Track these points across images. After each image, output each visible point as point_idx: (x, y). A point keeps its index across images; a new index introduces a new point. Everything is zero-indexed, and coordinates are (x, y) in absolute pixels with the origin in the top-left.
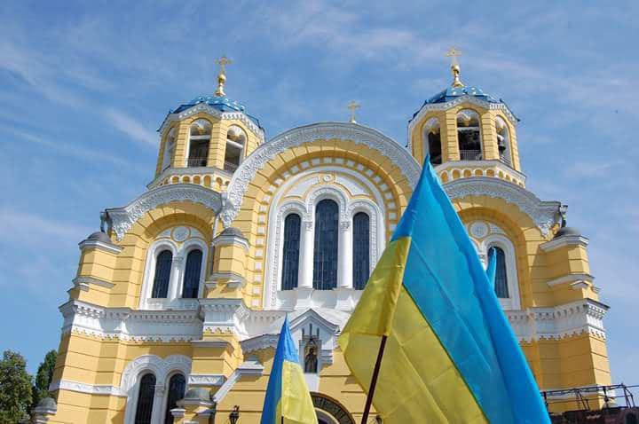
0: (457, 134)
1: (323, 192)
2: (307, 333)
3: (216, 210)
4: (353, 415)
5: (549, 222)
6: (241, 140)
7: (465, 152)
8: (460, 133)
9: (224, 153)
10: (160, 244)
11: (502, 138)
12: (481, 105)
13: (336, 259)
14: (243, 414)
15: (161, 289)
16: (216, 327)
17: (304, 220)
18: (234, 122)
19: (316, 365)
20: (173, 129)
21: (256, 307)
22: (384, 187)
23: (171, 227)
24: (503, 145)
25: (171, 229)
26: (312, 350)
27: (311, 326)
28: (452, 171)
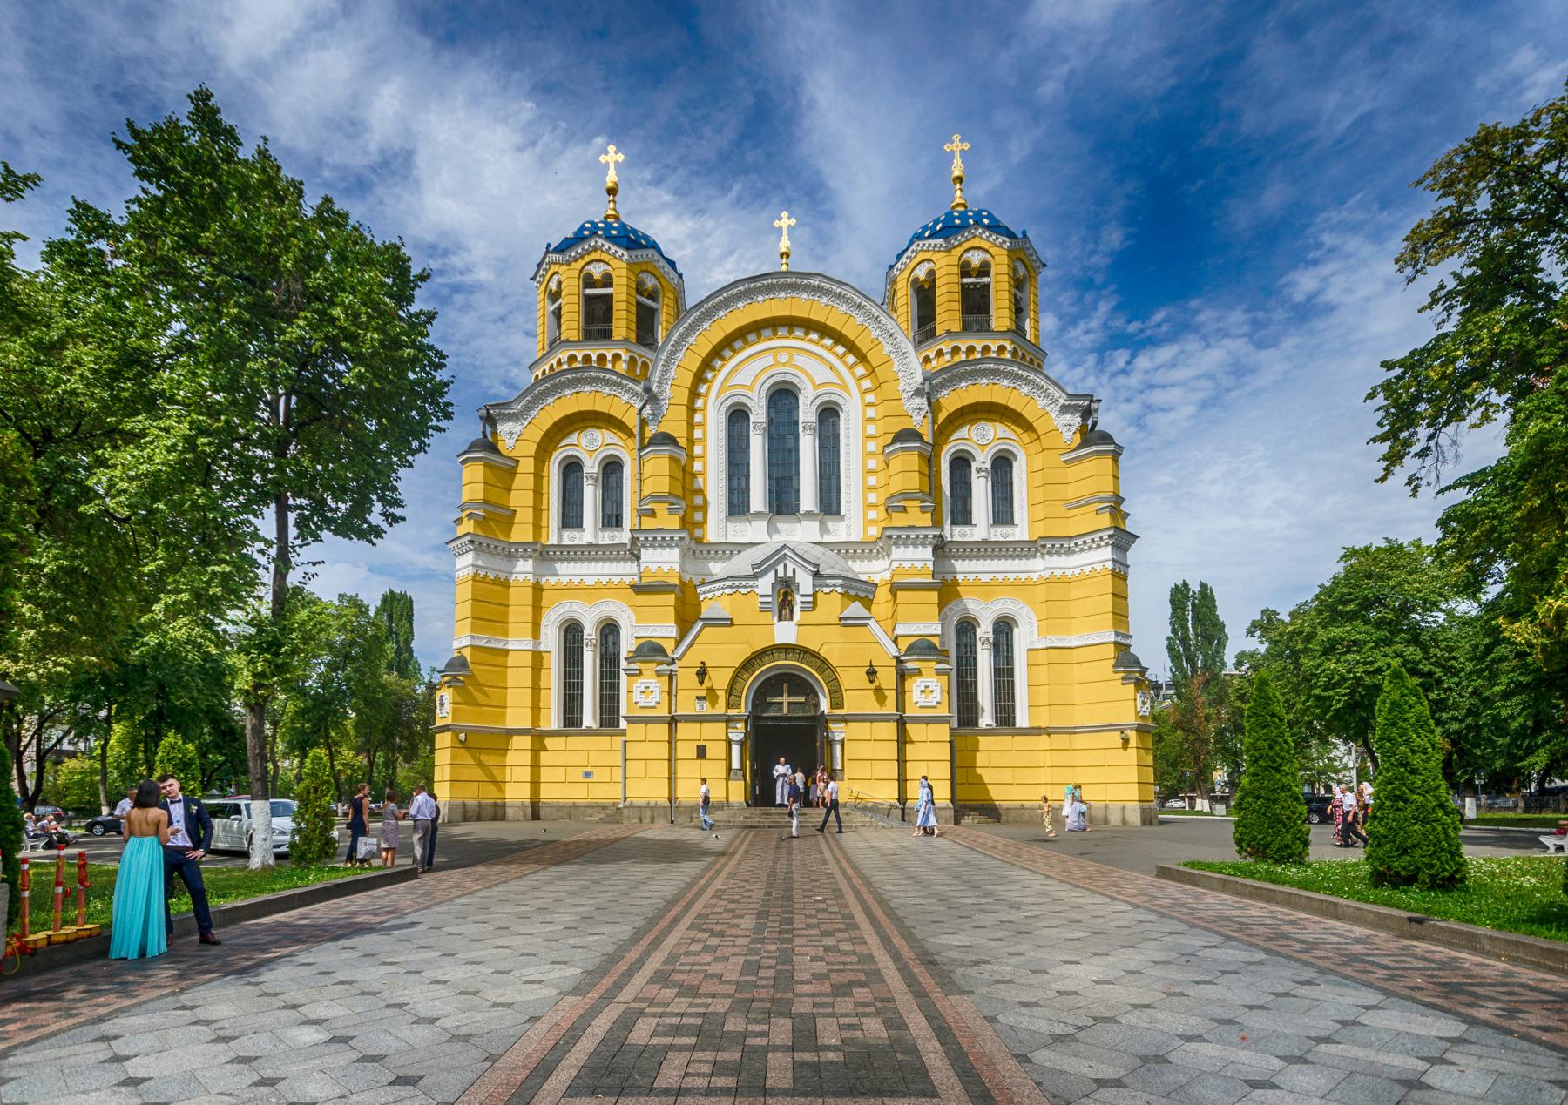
0: (957, 288)
2: (781, 574)
3: (638, 406)
5: (1077, 420)
6: (653, 296)
7: (969, 317)
8: (966, 291)
10: (564, 455)
11: (1019, 294)
13: (798, 474)
15: (571, 518)
16: (656, 566)
17: (752, 419)
18: (644, 268)
19: (792, 611)
20: (556, 277)
22: (860, 370)
23: (576, 430)
26: (786, 594)
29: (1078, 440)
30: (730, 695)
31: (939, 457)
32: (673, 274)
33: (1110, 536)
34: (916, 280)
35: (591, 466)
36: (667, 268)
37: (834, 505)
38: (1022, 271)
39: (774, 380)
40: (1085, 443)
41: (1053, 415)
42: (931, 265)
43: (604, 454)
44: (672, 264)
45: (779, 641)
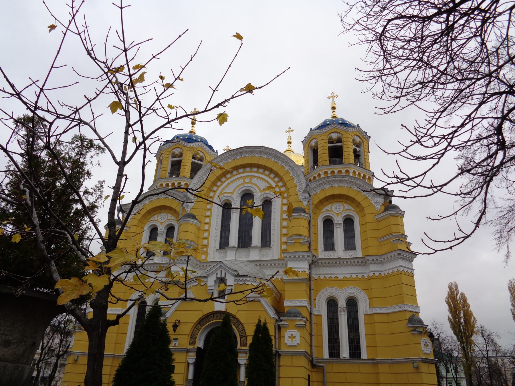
1: (245, 188)
2: (219, 276)
4: (244, 325)
8: (330, 148)
9: (190, 168)
10: (151, 224)
11: (358, 149)
12: (343, 129)
13: (251, 229)
14: (182, 324)
21: (204, 260)
22: (280, 184)
24: (358, 154)
25: (158, 214)
27: (221, 271)
28: (323, 172)
29: (383, 208)
30: (191, 338)
31: (316, 219)
32: (210, 151)
33: (399, 254)
34: (311, 147)
35: (162, 229)
36: (208, 149)
37: (268, 243)
38: (358, 140)
39: (242, 189)
40: (386, 209)
41: (370, 198)
42: (317, 140)
43: (167, 223)
44: (210, 147)
45: (216, 310)
